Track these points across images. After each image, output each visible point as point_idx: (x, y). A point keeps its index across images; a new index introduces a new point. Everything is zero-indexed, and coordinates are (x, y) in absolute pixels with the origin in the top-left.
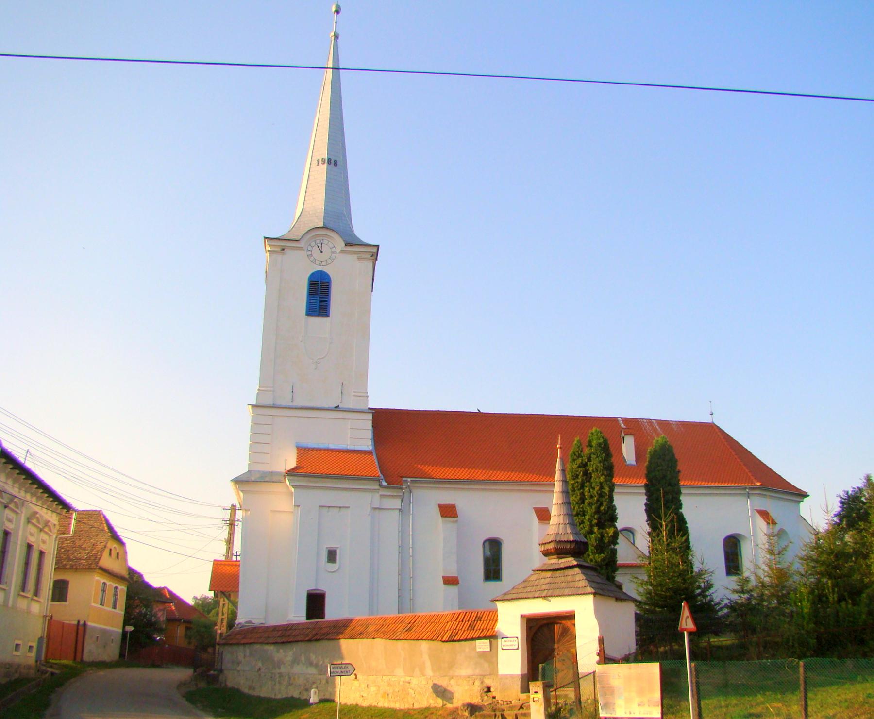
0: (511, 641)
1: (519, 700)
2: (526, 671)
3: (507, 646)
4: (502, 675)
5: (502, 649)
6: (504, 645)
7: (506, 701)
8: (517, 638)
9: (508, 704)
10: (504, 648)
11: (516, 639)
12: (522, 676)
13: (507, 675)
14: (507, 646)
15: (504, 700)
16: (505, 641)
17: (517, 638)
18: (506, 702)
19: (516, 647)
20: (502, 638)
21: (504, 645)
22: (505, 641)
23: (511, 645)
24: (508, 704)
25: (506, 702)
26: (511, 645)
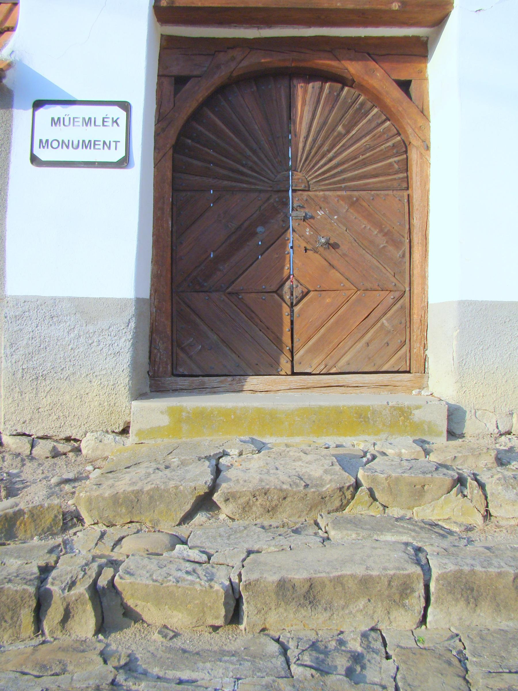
0: (88, 122)
1: (125, 431)
2: (146, 294)
3: (64, 144)
4: (18, 301)
5: (34, 159)
6: (45, 144)
7: (45, 438)
8: (125, 106)
9: (56, 454)
10: (43, 155)
11: (120, 114)
12: (139, 301)
13: (55, 301)
14: (64, 144)
15: (36, 431)
16: (55, 122)
17: (125, 106)
18: (49, 445)
19: (119, 154)
20: (38, 104)
21: (45, 144)
22: (55, 122)
23: (87, 145)
24: (56, 454)
25: (49, 445)
26: (87, 145)
